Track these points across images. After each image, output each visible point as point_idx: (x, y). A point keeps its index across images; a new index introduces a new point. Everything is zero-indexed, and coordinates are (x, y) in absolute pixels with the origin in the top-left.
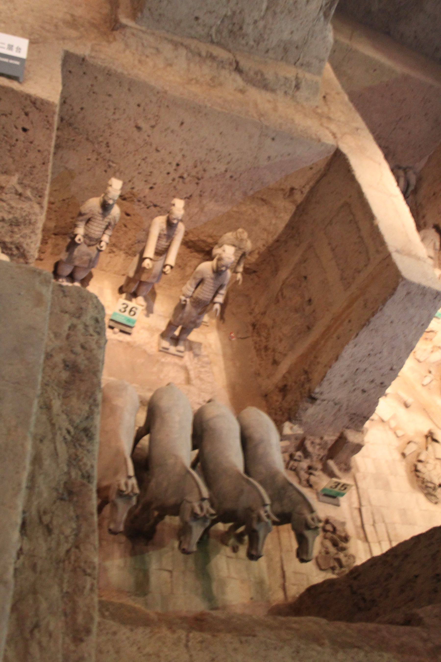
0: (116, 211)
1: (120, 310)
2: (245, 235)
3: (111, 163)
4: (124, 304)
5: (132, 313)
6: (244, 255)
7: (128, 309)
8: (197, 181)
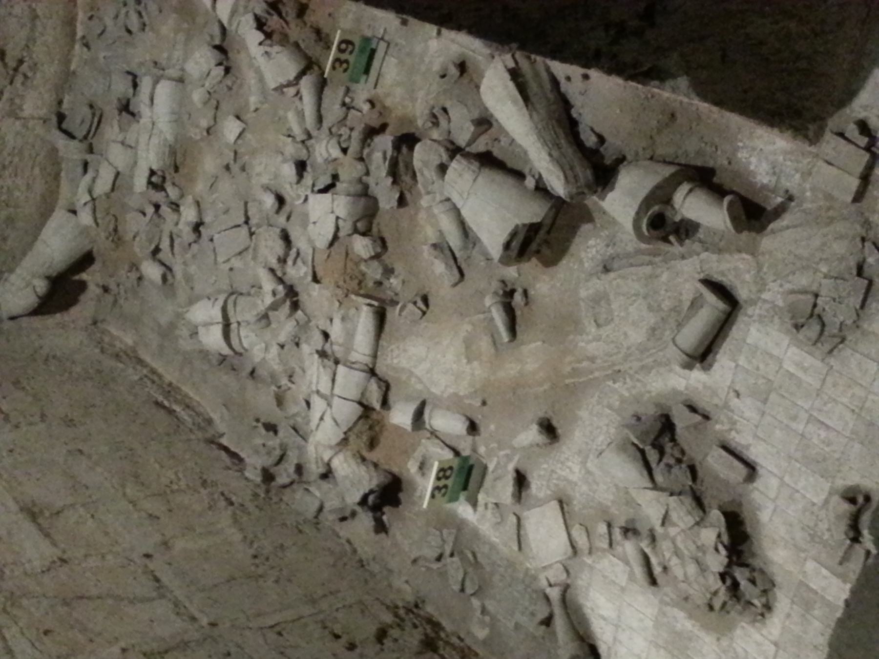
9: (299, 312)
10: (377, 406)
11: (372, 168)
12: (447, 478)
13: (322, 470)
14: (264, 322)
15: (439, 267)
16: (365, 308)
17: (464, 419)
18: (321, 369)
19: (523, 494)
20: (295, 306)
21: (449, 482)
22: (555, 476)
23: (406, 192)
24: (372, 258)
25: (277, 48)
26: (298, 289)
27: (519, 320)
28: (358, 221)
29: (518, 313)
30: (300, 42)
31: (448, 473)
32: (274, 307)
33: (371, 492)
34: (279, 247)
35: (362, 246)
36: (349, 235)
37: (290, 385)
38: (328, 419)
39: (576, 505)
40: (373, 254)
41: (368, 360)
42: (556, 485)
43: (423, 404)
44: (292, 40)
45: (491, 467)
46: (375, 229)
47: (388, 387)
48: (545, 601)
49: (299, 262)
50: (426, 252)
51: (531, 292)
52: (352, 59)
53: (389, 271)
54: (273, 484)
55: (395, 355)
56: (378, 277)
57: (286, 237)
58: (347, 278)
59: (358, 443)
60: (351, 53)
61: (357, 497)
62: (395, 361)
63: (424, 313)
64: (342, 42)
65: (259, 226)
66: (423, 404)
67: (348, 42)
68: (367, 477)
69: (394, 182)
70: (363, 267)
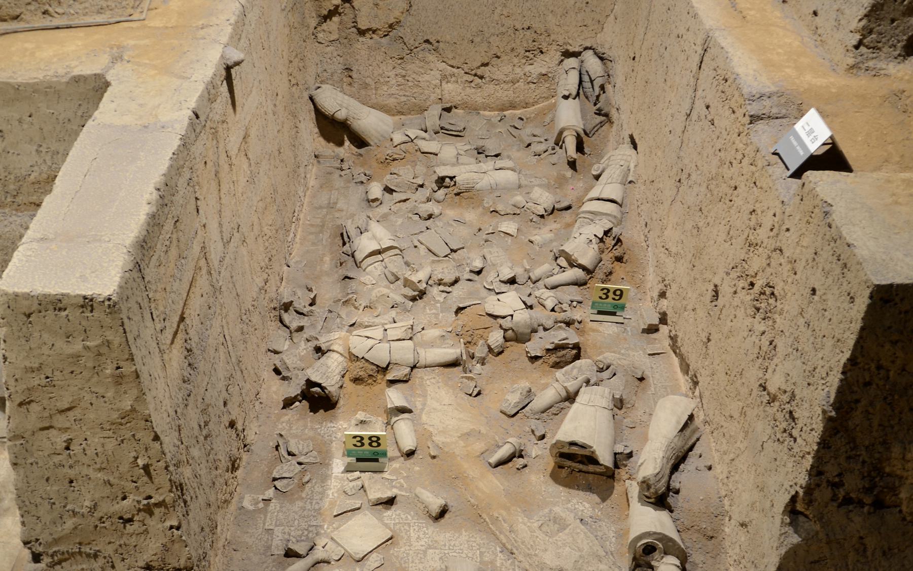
9: (411, 303)
10: (390, 377)
11: (552, 332)
12: (370, 444)
13: (324, 347)
14: (392, 278)
15: (513, 399)
16: (458, 351)
17: (415, 445)
18: (405, 328)
19: (380, 507)
20: (413, 299)
21: (367, 447)
22: (407, 528)
23: (541, 361)
24: (489, 347)
25: (596, 247)
26: (425, 298)
27: (506, 466)
28: (513, 330)
29: (510, 464)
30: (602, 262)
31: (375, 444)
32: (407, 283)
33: (323, 388)
34: (449, 278)
35: (496, 338)
36: (501, 326)
37: (361, 308)
38: (370, 342)
39: (394, 551)
40: (492, 347)
41: (422, 362)
42: (400, 529)
43: (410, 411)
44: (602, 256)
45: (386, 475)
46: (508, 344)
47: (406, 381)
48: (309, 548)
49: (444, 295)
50: (524, 384)
51: (527, 470)
52: (610, 300)
53: (483, 362)
54: (282, 312)
55: (433, 380)
56: (477, 355)
57: (456, 281)
58: (470, 333)
59: (357, 369)
60: (614, 299)
61: (315, 378)
62: (428, 382)
63: (470, 395)
64: (621, 291)
65: (454, 259)
66: (410, 411)
67: (621, 296)
68: (333, 383)
69: (548, 350)
70: (481, 342)
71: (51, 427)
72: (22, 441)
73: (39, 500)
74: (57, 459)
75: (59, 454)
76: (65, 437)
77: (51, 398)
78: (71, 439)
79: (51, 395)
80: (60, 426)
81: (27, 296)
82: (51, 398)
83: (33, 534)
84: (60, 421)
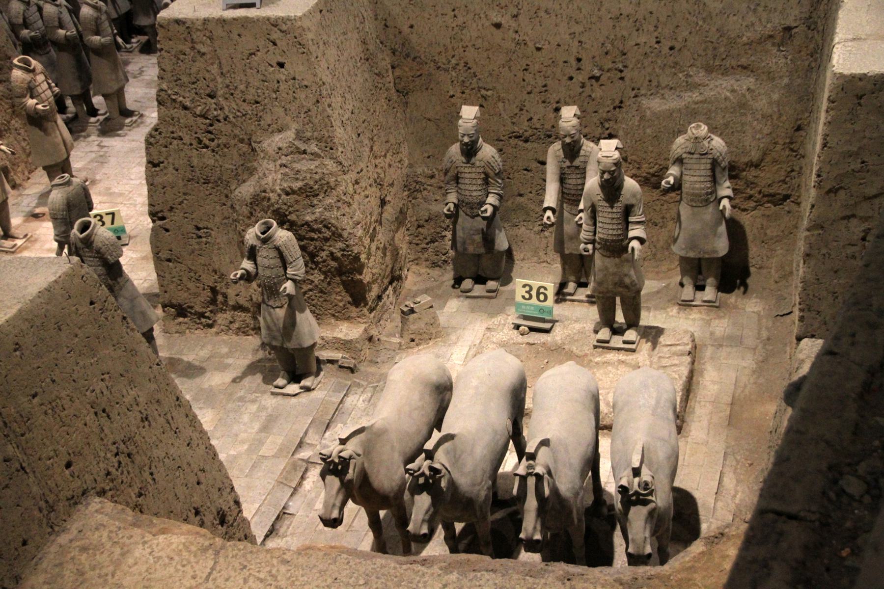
0: (487, 151)
1: (523, 297)
2: (704, 129)
3: (483, 92)
4: (524, 286)
5: (542, 297)
6: (715, 163)
7: (534, 293)
8: (619, 75)
71: (854, 216)
72: (821, 232)
73: (825, 293)
74: (850, 250)
75: (853, 245)
76: (865, 226)
77: (861, 184)
78: (869, 229)
79: (862, 181)
80: (862, 214)
81: (862, 78)
82: (861, 184)
83: (810, 330)
84: (863, 210)
